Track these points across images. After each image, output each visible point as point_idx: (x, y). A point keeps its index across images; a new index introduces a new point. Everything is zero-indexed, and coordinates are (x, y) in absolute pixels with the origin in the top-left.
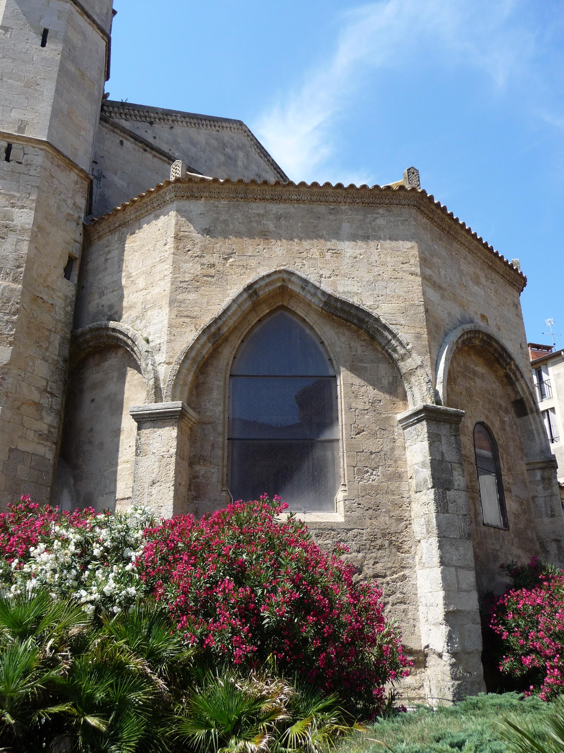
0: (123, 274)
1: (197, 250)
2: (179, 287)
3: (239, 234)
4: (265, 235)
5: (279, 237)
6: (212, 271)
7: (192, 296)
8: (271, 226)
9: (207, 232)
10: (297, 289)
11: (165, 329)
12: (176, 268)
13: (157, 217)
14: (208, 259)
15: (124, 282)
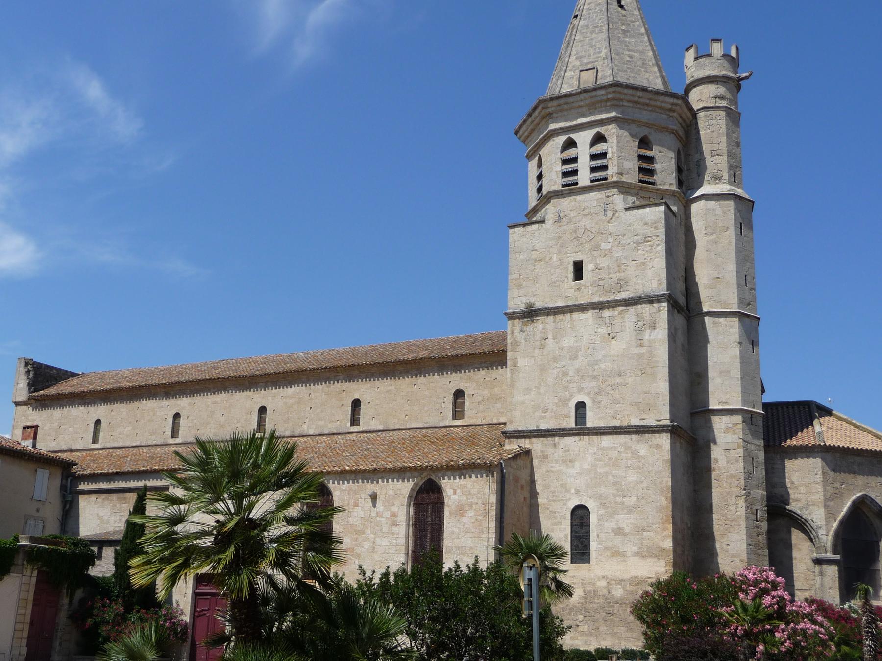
0: (787, 480)
1: (830, 481)
2: (828, 499)
3: (845, 472)
4: (854, 473)
5: (859, 474)
6: (837, 491)
7: (832, 503)
8: (856, 468)
9: (834, 470)
10: (868, 502)
11: (824, 519)
12: (825, 491)
13: (808, 457)
14: (837, 485)
15: (788, 485)
